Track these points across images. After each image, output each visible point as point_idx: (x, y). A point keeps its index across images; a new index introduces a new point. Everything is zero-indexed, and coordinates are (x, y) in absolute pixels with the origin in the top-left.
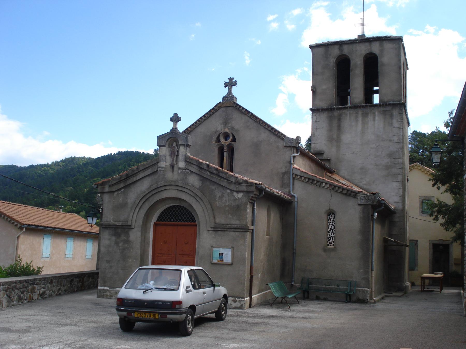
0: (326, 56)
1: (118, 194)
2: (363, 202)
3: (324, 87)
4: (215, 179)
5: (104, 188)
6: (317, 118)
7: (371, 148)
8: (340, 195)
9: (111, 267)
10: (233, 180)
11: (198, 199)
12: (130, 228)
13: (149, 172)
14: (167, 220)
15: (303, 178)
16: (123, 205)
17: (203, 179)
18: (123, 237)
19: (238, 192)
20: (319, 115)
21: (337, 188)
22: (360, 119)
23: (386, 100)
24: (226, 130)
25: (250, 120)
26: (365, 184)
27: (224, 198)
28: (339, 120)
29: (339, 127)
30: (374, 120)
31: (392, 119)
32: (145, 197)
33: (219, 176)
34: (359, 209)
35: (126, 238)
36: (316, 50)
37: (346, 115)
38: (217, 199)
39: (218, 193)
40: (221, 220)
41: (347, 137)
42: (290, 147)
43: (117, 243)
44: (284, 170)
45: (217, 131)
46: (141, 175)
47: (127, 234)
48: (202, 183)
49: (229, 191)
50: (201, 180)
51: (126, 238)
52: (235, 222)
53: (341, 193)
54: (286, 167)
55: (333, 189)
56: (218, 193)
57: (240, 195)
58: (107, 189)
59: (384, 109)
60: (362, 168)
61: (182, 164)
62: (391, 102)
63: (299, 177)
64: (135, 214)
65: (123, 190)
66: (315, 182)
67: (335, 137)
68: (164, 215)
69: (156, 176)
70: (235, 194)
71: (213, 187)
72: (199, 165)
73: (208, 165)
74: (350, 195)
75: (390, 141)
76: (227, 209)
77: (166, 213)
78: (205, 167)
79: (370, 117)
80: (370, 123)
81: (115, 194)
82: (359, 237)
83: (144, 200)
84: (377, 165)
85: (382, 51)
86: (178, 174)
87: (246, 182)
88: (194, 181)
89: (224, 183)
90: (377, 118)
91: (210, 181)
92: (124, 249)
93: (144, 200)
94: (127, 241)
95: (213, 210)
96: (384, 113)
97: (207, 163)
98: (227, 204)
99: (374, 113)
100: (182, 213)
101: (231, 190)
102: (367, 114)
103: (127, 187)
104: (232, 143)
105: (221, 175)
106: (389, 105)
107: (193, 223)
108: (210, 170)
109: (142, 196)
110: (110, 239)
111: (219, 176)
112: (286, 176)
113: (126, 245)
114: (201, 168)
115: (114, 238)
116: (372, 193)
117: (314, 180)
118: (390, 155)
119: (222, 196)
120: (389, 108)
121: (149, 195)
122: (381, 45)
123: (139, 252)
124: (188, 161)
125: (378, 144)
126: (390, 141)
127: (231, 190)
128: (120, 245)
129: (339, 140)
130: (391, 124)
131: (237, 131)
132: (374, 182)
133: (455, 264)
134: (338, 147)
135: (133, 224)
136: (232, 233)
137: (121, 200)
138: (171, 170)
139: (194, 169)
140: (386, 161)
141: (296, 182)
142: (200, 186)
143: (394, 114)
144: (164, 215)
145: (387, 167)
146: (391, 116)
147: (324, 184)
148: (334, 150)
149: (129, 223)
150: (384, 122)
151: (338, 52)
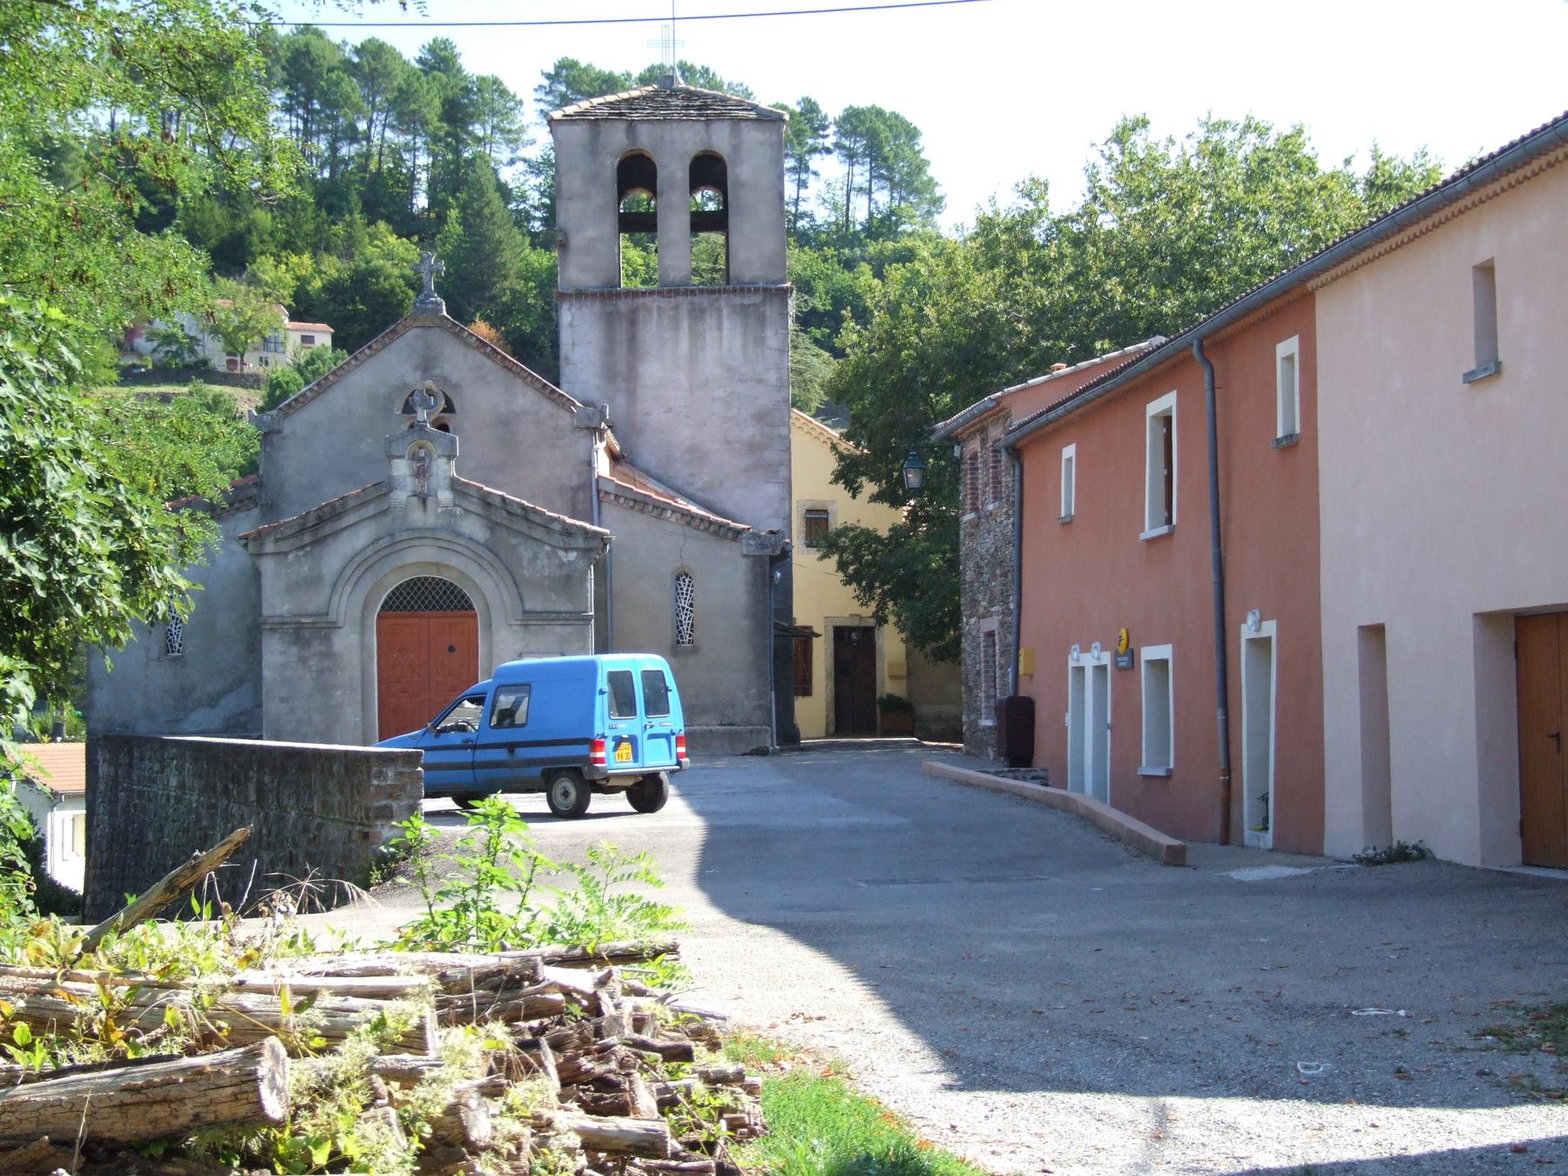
0: (594, 147)
1: (297, 556)
2: (752, 551)
3: (591, 233)
4: (521, 526)
5: (262, 545)
6: (573, 317)
7: (713, 399)
8: (703, 535)
9: (292, 710)
10: (557, 527)
11: (485, 564)
12: (334, 626)
13: (370, 510)
14: (405, 607)
15: (622, 500)
16: (314, 581)
17: (493, 526)
18: (317, 647)
19: (567, 550)
20: (580, 308)
21: (697, 522)
22: (685, 324)
23: (747, 278)
24: (429, 383)
25: (488, 362)
26: (699, 489)
27: (539, 562)
28: (633, 323)
29: (632, 340)
30: (720, 328)
31: (763, 331)
32: (363, 564)
33: (527, 520)
34: (744, 564)
35: (323, 648)
36: (564, 130)
37: (649, 310)
38: (525, 563)
39: (525, 552)
40: (534, 603)
41: (651, 370)
42: (587, 428)
43: (303, 660)
44: (575, 481)
45: (405, 386)
46: (352, 518)
47: (327, 639)
48: (492, 533)
49: (548, 548)
50: (488, 527)
51: (323, 648)
52: (563, 605)
53: (706, 530)
54: (580, 475)
55: (689, 524)
56: (525, 552)
57: (572, 556)
58: (270, 547)
59: (746, 301)
60: (692, 450)
61: (445, 496)
62: (761, 285)
63: (612, 497)
64: (344, 599)
65: (308, 549)
66: (651, 508)
67: (622, 367)
68: (398, 598)
69: (387, 520)
70: (561, 553)
71: (514, 541)
72: (485, 500)
73: (503, 499)
74: (725, 536)
75: (760, 381)
76: (547, 582)
77: (401, 594)
78: (497, 502)
79: (710, 321)
80: (710, 336)
81: (291, 557)
82: (746, 623)
83: (362, 569)
84: (728, 442)
85: (736, 148)
86: (438, 516)
87: (585, 532)
88: (473, 527)
89: (539, 533)
90: (726, 324)
91: (508, 528)
92: (321, 672)
93: (362, 569)
94: (329, 655)
95: (517, 587)
96: (743, 311)
97: (500, 493)
98: (546, 574)
99: (719, 311)
100: (437, 593)
101: (554, 547)
102: (702, 310)
103: (318, 542)
104: (446, 415)
105: (532, 517)
106: (757, 290)
107: (463, 612)
108: (509, 508)
109: (358, 560)
110: (284, 653)
111: (527, 520)
112: (581, 495)
113: (326, 664)
114: (489, 504)
115: (294, 650)
116: (772, 532)
117: (645, 504)
118: (760, 418)
119: (535, 558)
120: (757, 299)
121: (374, 559)
122: (735, 132)
123: (357, 674)
124: (454, 485)
125: (729, 390)
126: (760, 381)
127: (554, 547)
128: (312, 663)
129: (632, 377)
130: (760, 341)
131: (457, 387)
132: (721, 484)
133: (892, 677)
134: (632, 395)
135: (342, 618)
136: (558, 629)
137: (305, 568)
138: (421, 508)
139: (474, 506)
140: (751, 432)
141: (605, 507)
142: (486, 540)
143: (768, 313)
144: (398, 598)
145: (753, 448)
146: (762, 320)
147: (669, 513)
148: (621, 401)
149: (332, 617)
150: (745, 334)
151: (626, 142)
